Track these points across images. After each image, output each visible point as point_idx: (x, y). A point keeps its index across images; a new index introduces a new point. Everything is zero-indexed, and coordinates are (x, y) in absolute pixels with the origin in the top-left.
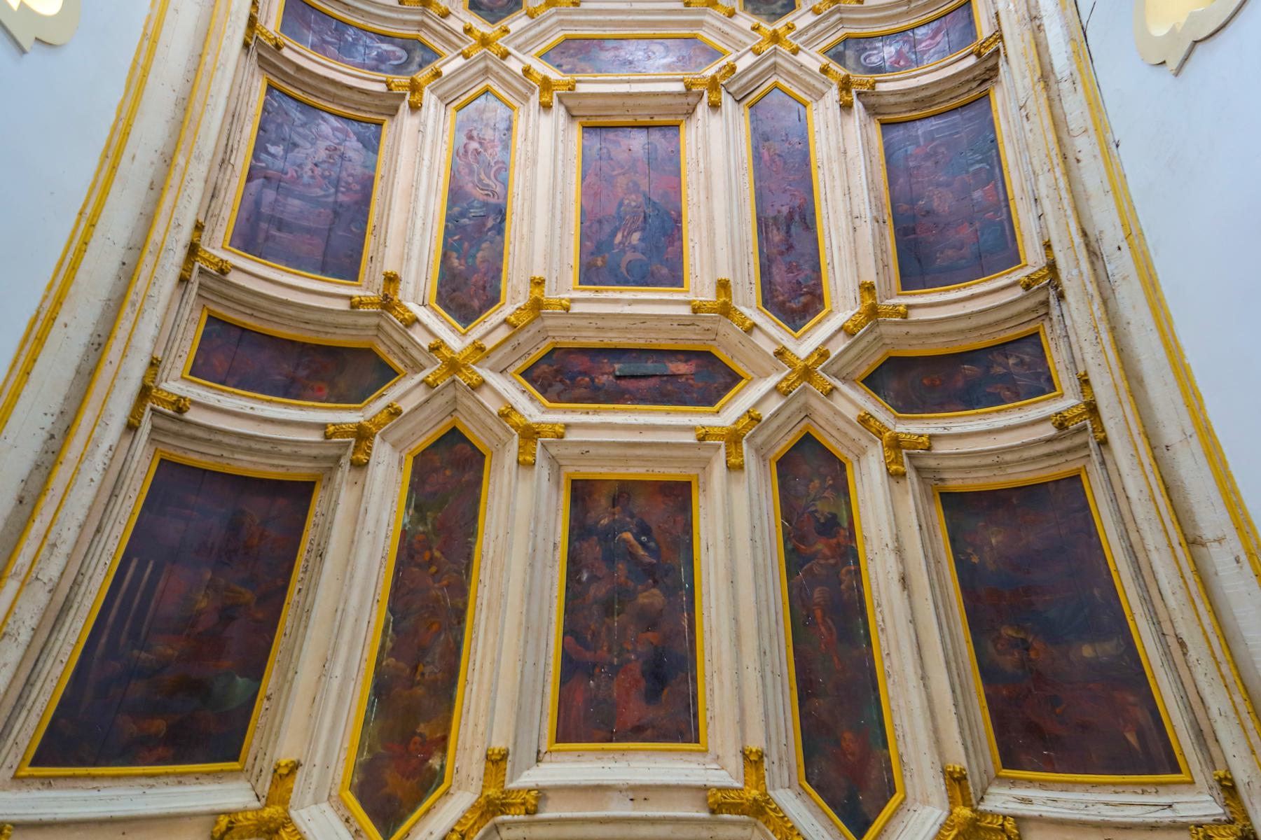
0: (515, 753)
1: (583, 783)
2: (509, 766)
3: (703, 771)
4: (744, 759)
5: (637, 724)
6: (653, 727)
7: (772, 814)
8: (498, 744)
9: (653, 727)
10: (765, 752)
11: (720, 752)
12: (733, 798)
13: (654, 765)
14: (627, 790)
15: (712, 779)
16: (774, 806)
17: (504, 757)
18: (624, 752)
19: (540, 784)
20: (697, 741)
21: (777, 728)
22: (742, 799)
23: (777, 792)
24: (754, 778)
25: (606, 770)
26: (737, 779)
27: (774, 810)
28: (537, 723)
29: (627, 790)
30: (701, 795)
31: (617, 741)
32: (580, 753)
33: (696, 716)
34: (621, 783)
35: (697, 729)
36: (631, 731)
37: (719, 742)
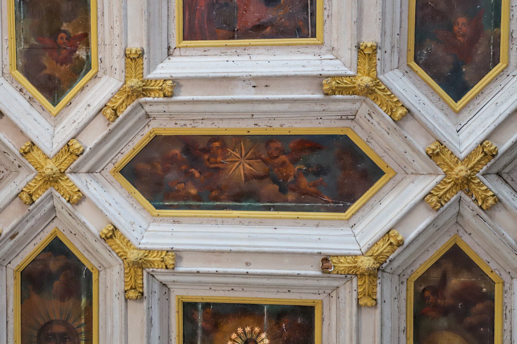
0: (149, 53)
1: (211, 75)
2: (145, 62)
3: (319, 62)
4: (359, 52)
5: (258, 23)
6: (272, 26)
7: (380, 93)
8: (134, 46)
9: (272, 26)
10: (379, 45)
11: (335, 44)
12: (346, 83)
13: (272, 58)
14: (249, 80)
15: (326, 69)
16: (383, 87)
17: (141, 55)
18: (245, 47)
19: (174, 75)
20: (314, 36)
21: (393, 20)
22: (354, 83)
23: (386, 75)
24: (367, 67)
25: (230, 63)
26: (350, 68)
27: (383, 90)
28: (165, 25)
29: (249, 80)
30: (317, 81)
31: (239, 38)
32: (206, 49)
33: (313, 14)
34: (244, 74)
35: (314, 26)
36: (251, 29)
37: (335, 36)
